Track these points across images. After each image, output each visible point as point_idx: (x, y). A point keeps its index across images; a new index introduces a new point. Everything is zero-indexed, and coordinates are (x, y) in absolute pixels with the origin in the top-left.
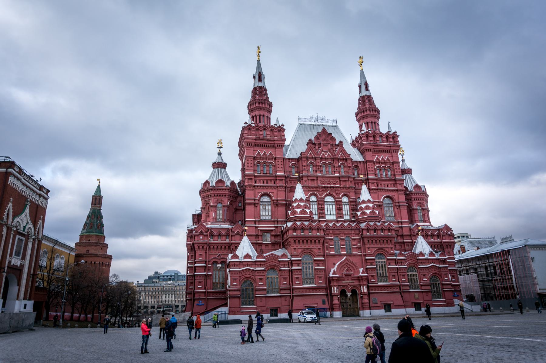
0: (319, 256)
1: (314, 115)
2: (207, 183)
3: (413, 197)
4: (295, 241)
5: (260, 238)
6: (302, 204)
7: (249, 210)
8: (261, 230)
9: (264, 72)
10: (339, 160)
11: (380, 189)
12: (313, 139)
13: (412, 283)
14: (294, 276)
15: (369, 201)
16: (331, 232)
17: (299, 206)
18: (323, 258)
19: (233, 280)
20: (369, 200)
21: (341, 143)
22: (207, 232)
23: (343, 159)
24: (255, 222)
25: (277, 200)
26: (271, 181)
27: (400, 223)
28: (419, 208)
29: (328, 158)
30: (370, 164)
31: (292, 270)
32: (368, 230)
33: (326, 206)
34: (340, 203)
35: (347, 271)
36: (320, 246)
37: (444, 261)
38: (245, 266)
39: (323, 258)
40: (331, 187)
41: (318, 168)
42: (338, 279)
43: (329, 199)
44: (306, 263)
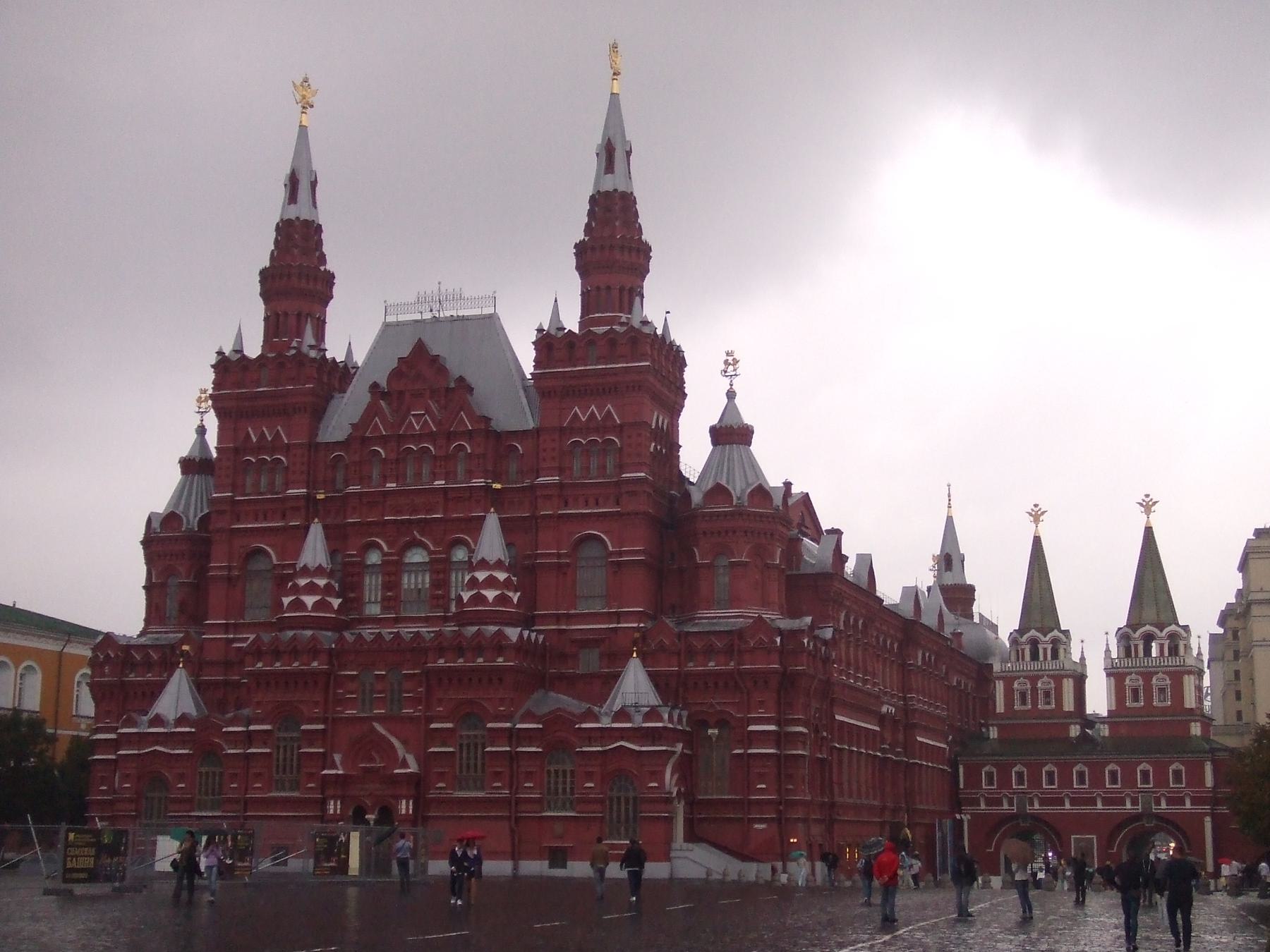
0: (311, 721)
1: (430, 288)
2: (149, 521)
6: (302, 582)
9: (319, 164)
10: (450, 437)
12: (383, 383)
13: (557, 793)
14: (253, 771)
15: (484, 564)
17: (296, 590)
18: (321, 727)
21: (461, 380)
22: (117, 656)
23: (463, 433)
24: (226, 628)
28: (723, 561)
31: (248, 757)
32: (441, 651)
33: (405, 580)
34: (440, 567)
35: (372, 760)
39: (321, 727)
43: (417, 556)
44: (285, 739)
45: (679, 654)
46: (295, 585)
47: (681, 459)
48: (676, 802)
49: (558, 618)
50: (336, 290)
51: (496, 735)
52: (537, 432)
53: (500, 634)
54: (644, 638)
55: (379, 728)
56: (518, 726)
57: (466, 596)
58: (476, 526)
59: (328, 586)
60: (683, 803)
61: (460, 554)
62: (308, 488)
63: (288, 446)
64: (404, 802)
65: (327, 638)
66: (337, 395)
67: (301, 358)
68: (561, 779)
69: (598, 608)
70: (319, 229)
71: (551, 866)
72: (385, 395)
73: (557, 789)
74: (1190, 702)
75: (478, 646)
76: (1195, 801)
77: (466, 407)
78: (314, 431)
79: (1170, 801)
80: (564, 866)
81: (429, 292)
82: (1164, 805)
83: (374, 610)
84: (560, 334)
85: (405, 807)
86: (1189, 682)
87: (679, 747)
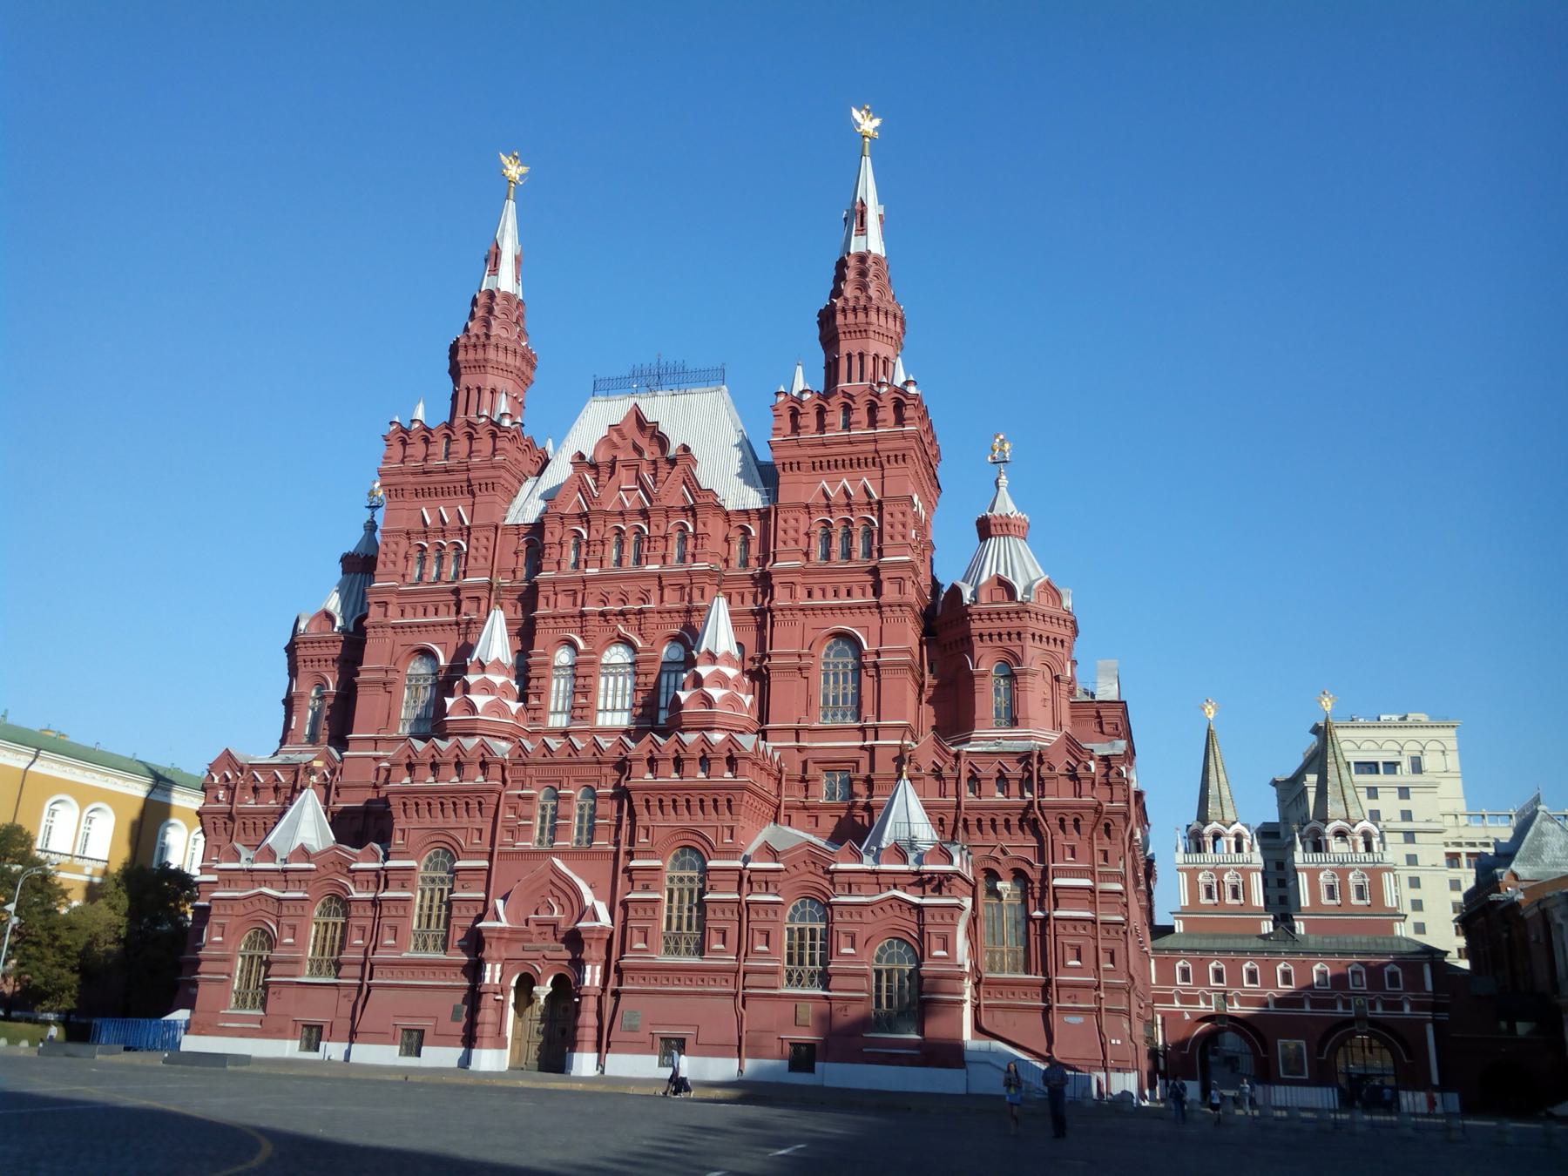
3: (976, 626)
13: (801, 963)
16: (531, 771)
20: (709, 653)
21: (686, 448)
27: (870, 733)
29: (631, 512)
30: (790, 516)
39: (485, 863)
49: (797, 731)
55: (558, 862)
59: (506, 685)
63: (468, 528)
74: (1390, 902)
76: (1415, 1006)
77: (691, 482)
79: (1386, 1006)
80: (811, 1070)
81: (646, 365)
82: (1379, 1010)
83: (558, 721)
86: (1387, 879)
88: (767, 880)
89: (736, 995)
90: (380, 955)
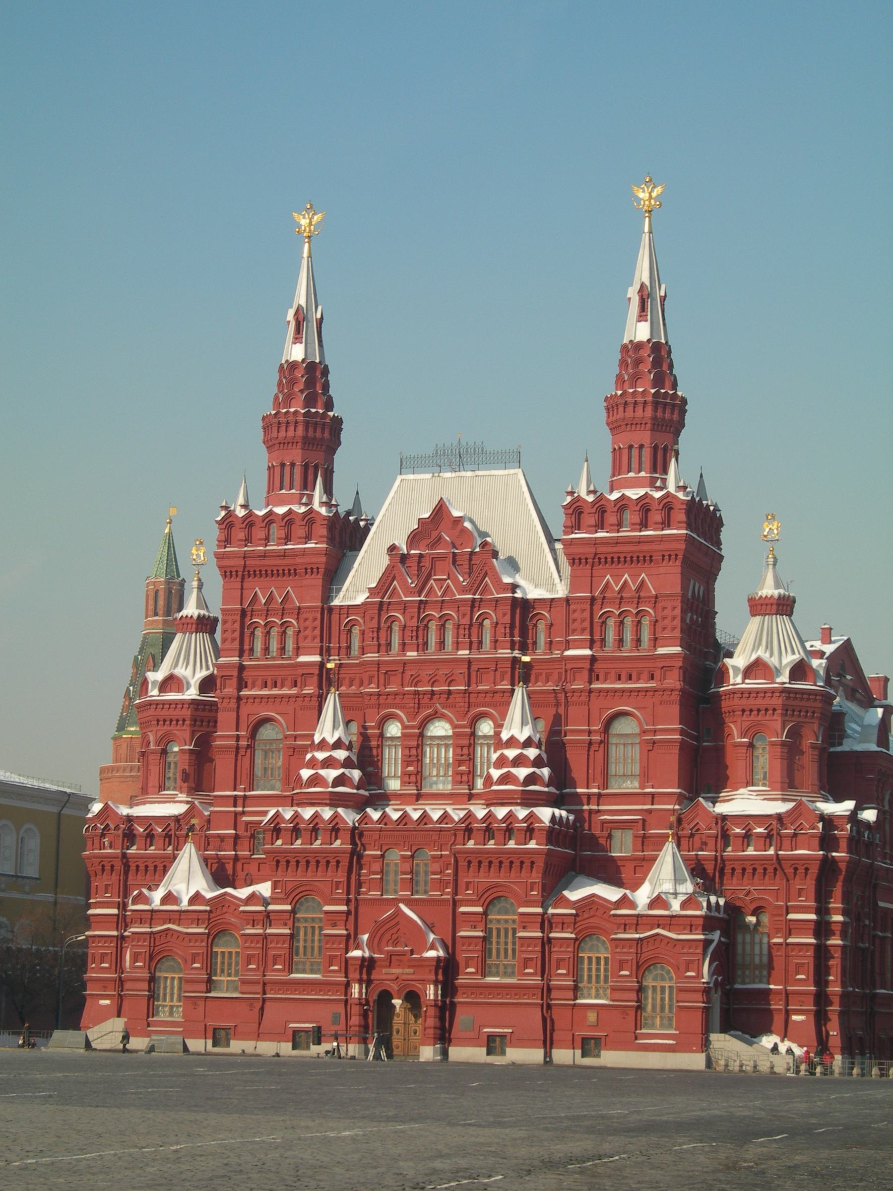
4: (278, 862)
5: (245, 843)
6: (321, 756)
7: (223, 766)
8: (247, 823)
11: (600, 691)
15: (512, 742)
17: (313, 764)
18: (344, 908)
19: (135, 957)
20: (512, 737)
22: (117, 828)
25: (295, 738)
26: (283, 680)
31: (265, 937)
32: (469, 832)
36: (341, 877)
37: (688, 924)
38: (164, 923)
39: (344, 908)
40: (441, 693)
41: (417, 635)
42: (368, 964)
43: (440, 729)
45: (717, 837)
46: (313, 757)
47: (718, 626)
48: (713, 992)
50: (343, 436)
51: (526, 921)
52: (567, 600)
53: (531, 815)
54: (679, 821)
56: (551, 911)
57: (496, 774)
58: (503, 702)
60: (719, 993)
61: (486, 728)
62: (321, 654)
63: (299, 608)
64: (432, 986)
65: (349, 817)
66: (349, 553)
67: (310, 517)
68: (594, 966)
69: (631, 786)
70: (325, 372)
71: (584, 1055)
72: (404, 558)
73: (590, 977)
75: (509, 828)
78: (327, 596)
80: (598, 1056)
84: (590, 498)
85: (431, 992)
87: (716, 936)
88: (562, 922)
89: (542, 1005)
90: (271, 976)
